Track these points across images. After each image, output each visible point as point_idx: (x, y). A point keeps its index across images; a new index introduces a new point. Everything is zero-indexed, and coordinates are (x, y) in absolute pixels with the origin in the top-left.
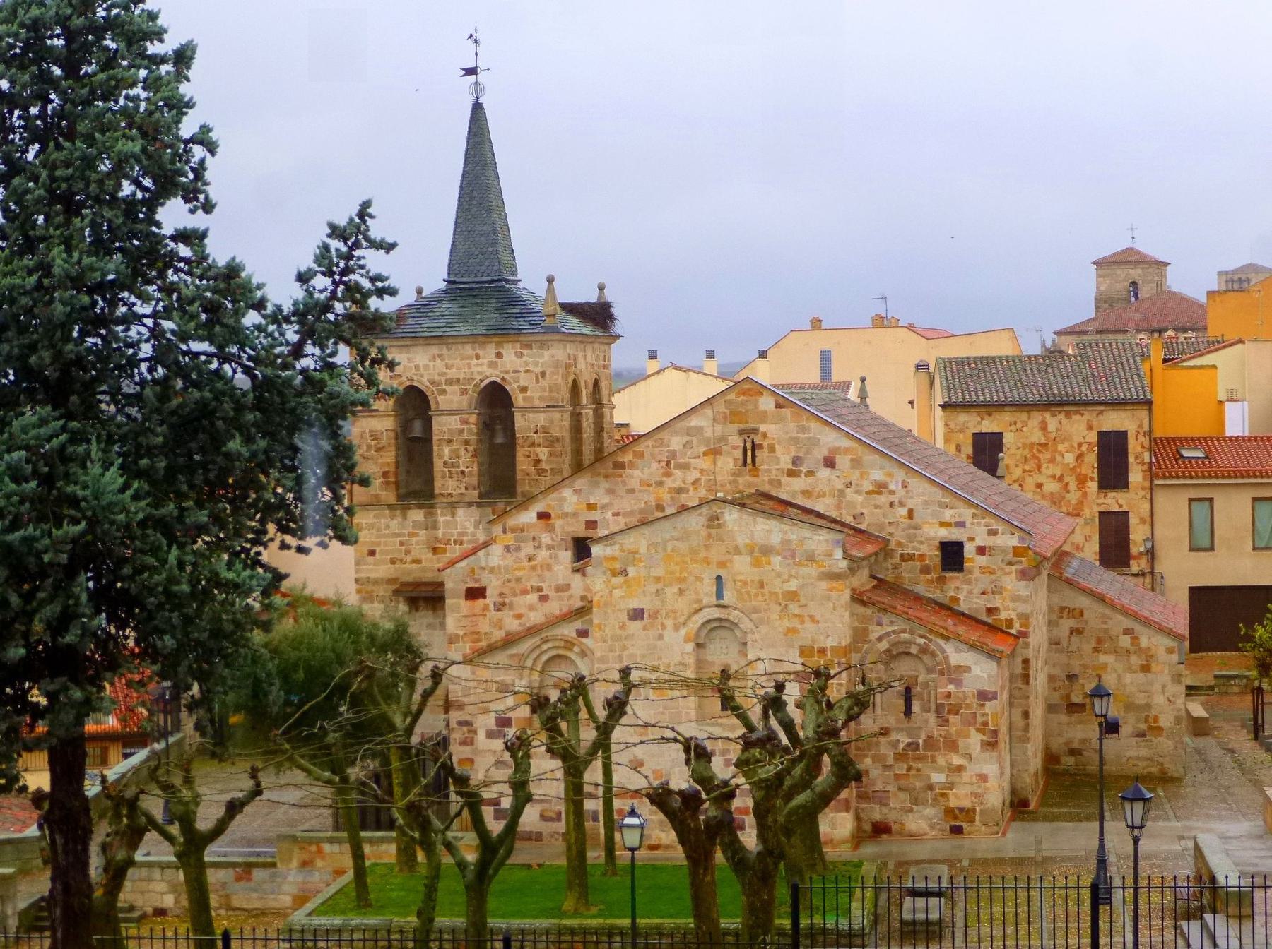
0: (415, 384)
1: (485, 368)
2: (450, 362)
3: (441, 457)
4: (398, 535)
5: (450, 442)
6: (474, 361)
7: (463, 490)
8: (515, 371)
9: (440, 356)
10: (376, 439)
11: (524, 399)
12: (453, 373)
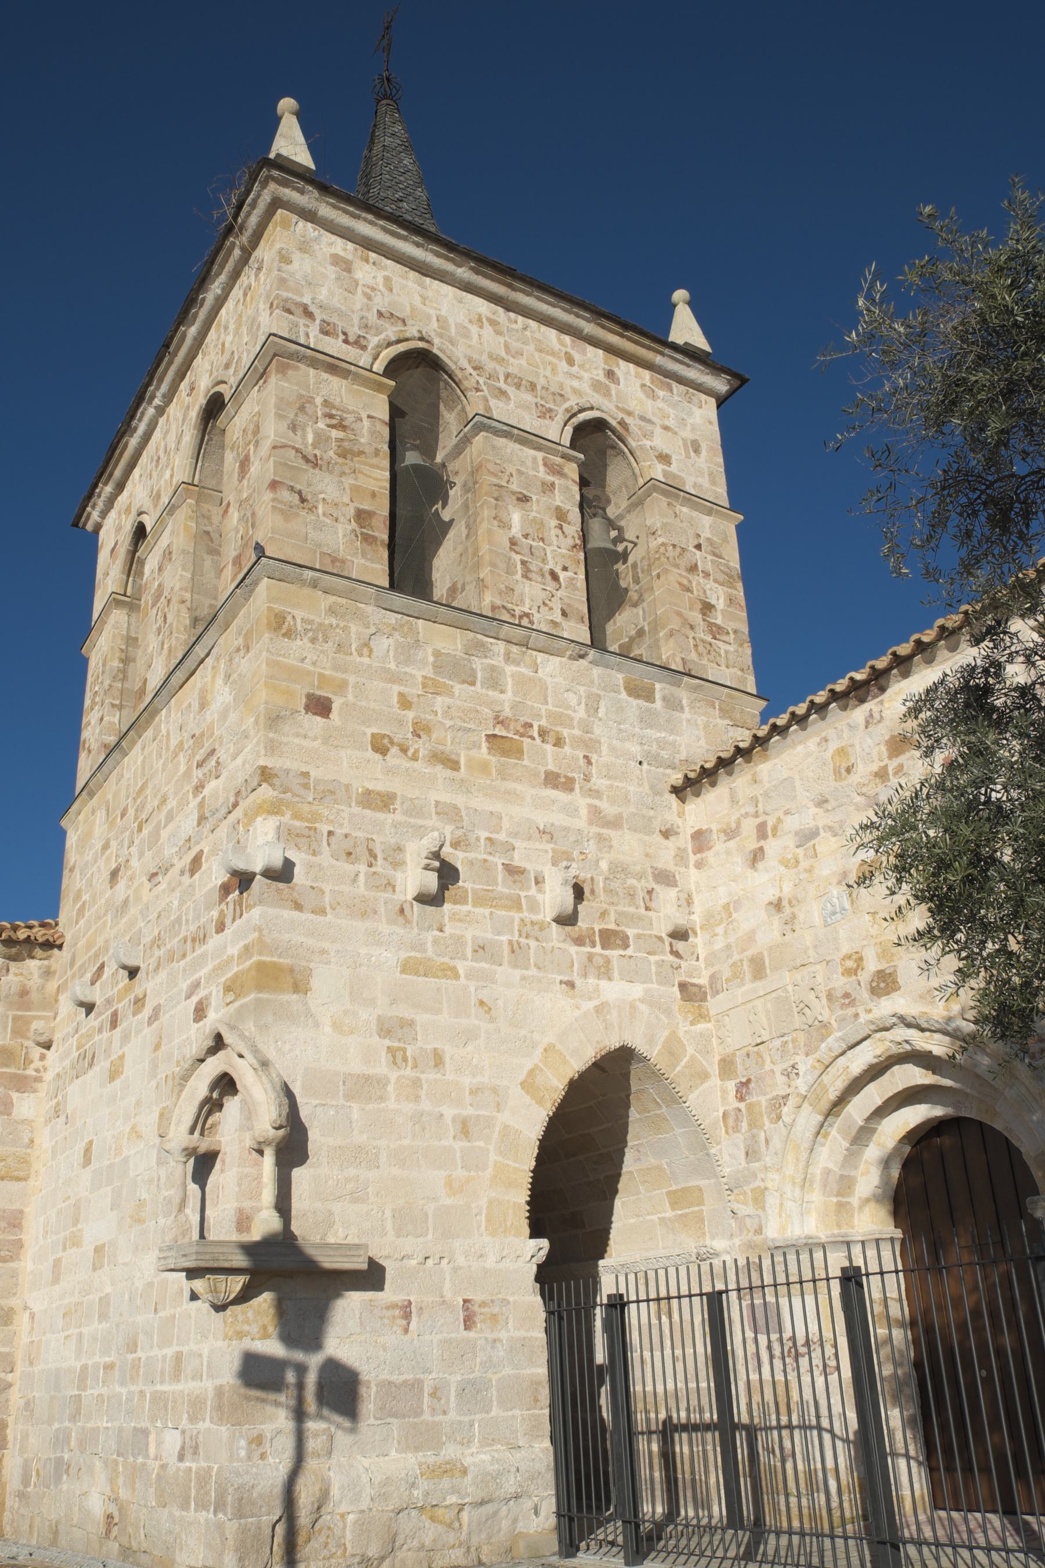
0: (435, 351)
1: (585, 387)
2: (515, 345)
3: (506, 525)
4: (394, 678)
5: (524, 499)
6: (563, 365)
7: (557, 616)
8: (643, 418)
9: (493, 323)
10: (341, 426)
11: (665, 474)
12: (516, 366)
